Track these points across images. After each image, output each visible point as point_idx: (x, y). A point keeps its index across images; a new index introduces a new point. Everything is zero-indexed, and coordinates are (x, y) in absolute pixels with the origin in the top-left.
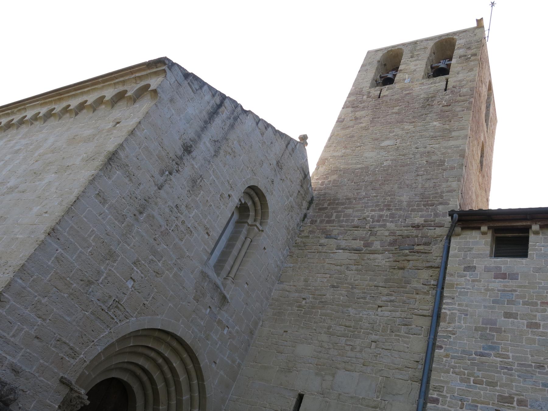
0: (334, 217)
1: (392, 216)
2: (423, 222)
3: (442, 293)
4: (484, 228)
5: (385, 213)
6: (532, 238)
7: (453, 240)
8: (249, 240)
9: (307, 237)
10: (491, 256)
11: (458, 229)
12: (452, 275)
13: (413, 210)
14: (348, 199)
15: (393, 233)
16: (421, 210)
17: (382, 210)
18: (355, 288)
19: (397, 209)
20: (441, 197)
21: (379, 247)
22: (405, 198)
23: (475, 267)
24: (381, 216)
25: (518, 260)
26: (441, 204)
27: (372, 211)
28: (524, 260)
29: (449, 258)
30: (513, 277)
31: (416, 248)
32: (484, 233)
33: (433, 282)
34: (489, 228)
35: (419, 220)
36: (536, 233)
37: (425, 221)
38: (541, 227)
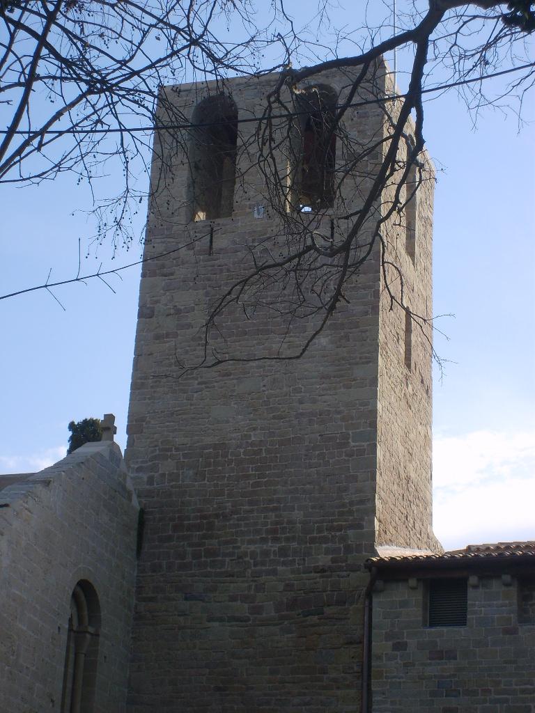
0: (189, 559)
1: (283, 552)
2: (330, 564)
3: (369, 685)
4: (412, 582)
5: (275, 547)
6: (471, 593)
7: (375, 600)
8: (82, 658)
9: (151, 599)
10: (424, 625)
11: (379, 584)
12: (379, 658)
13: (313, 540)
14: (204, 517)
15: (289, 587)
16: (325, 540)
17: (264, 540)
18: (252, 688)
19: (288, 539)
20: (351, 512)
21: (273, 614)
22: (298, 515)
23: (406, 644)
24: (266, 553)
25: (456, 629)
26: (351, 527)
27: (250, 542)
28: (462, 630)
29: (374, 631)
30: (448, 655)
31: (327, 610)
32: (414, 588)
33: (356, 669)
34: (418, 580)
35: (323, 560)
36: (475, 587)
37: (334, 560)
38: (481, 578)
